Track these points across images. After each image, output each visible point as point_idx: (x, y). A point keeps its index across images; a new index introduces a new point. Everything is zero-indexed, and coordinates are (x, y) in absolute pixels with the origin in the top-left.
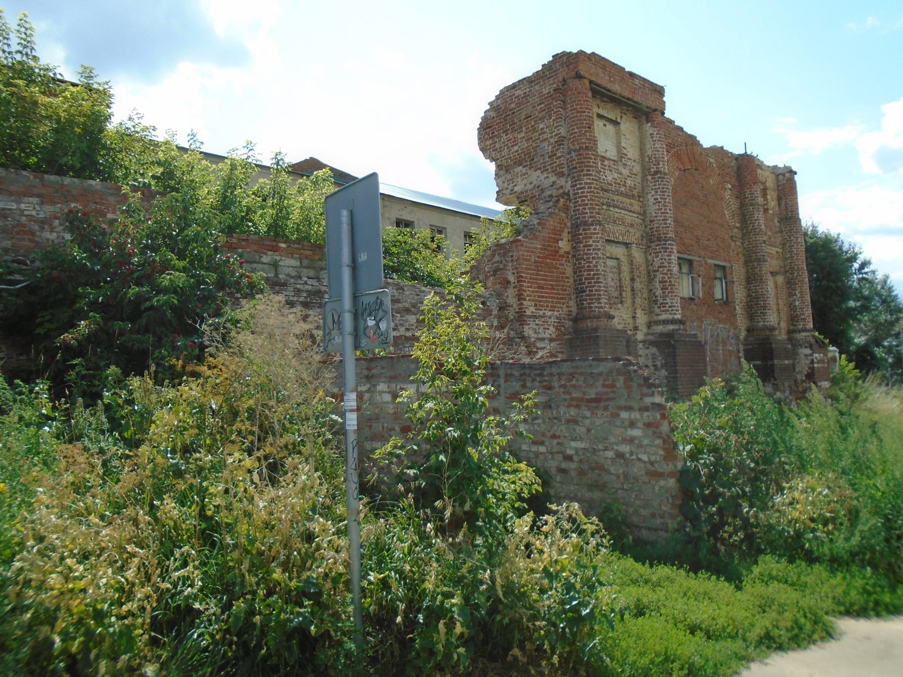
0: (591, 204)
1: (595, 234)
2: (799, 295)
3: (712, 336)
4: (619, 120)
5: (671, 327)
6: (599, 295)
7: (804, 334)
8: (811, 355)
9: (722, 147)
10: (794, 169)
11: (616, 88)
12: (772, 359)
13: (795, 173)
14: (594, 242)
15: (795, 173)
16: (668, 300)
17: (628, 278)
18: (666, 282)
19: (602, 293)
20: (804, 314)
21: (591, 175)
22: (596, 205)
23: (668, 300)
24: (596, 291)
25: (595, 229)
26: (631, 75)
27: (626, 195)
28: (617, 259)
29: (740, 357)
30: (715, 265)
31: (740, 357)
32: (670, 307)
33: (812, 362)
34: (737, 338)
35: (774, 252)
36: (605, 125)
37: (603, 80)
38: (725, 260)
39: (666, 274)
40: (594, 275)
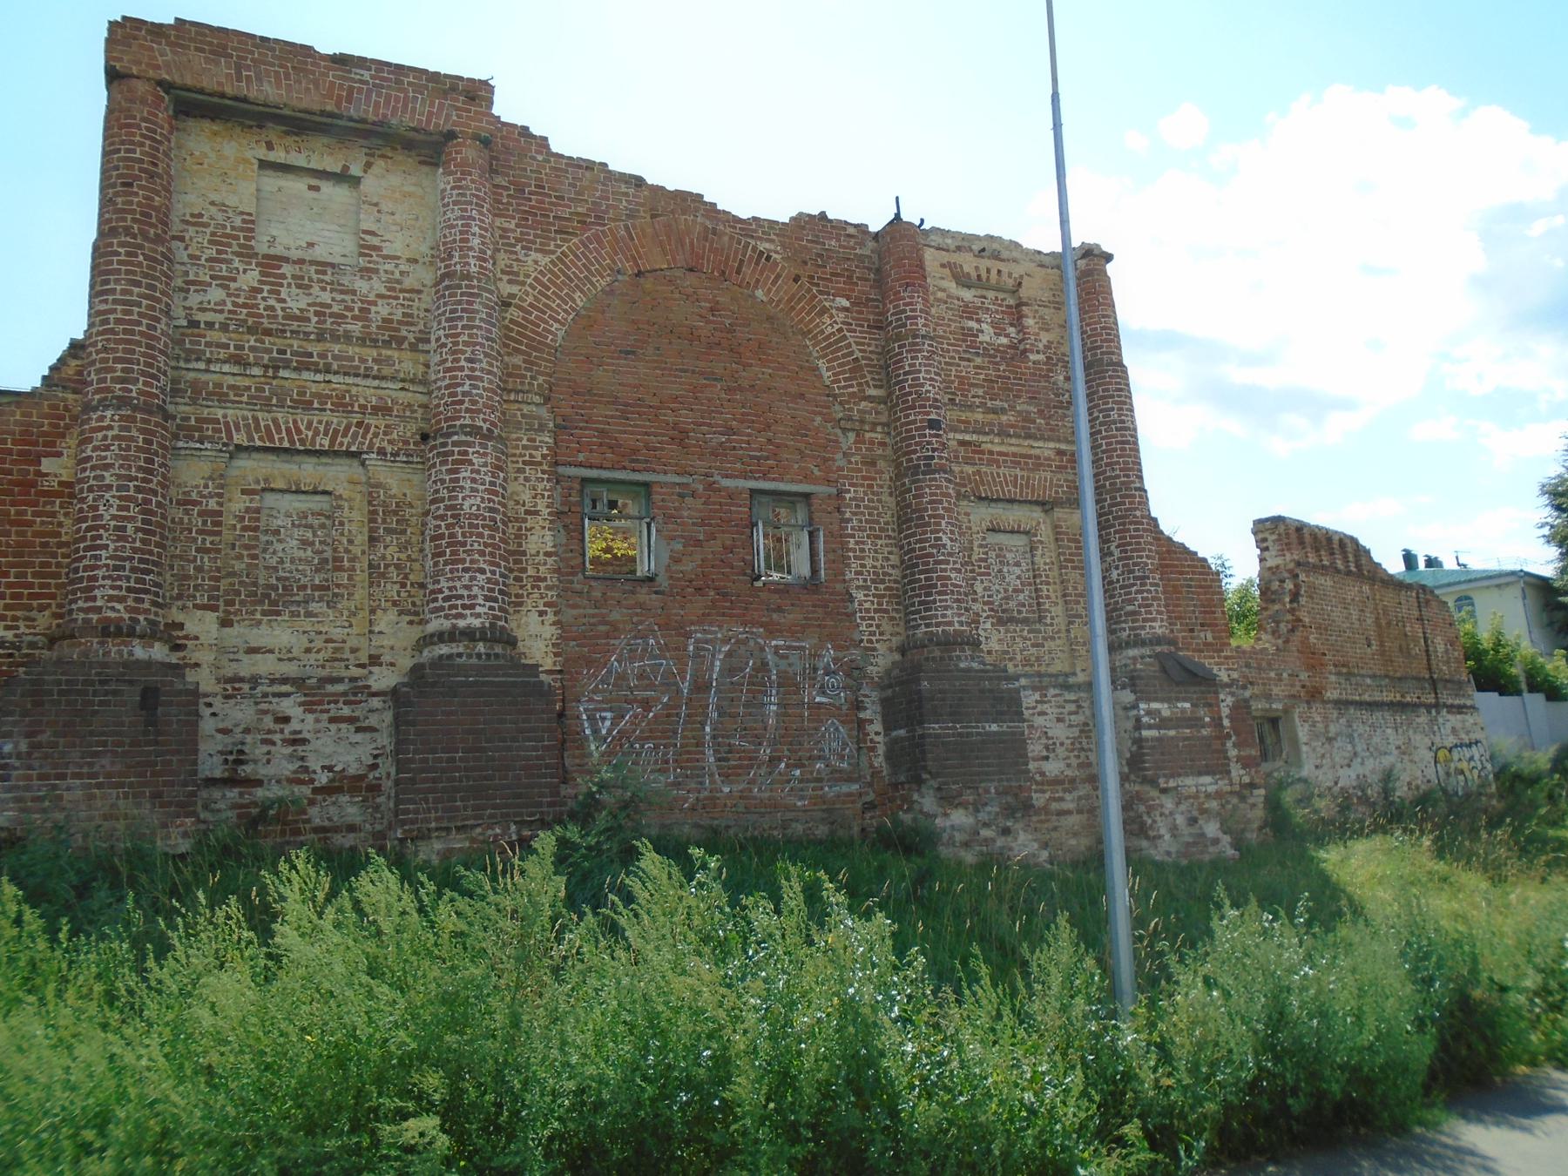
0: (106, 360)
1: (101, 429)
2: (1117, 553)
3: (730, 671)
4: (355, 170)
5: (444, 650)
6: (94, 578)
7: (1132, 652)
8: (1135, 707)
9: (823, 215)
10: (1106, 248)
11: (268, 91)
12: (921, 723)
13: (1108, 258)
14: (95, 449)
15: (1108, 258)
16: (444, 584)
17: (361, 538)
18: (442, 537)
19: (100, 573)
20: (1131, 602)
21: (113, 291)
22: (116, 360)
23: (444, 584)
24: (86, 569)
25: (102, 418)
26: (342, 60)
27: (365, 340)
28: (325, 493)
29: (861, 724)
30: (753, 492)
31: (861, 724)
32: (445, 599)
33: (1138, 725)
34: (854, 672)
35: (1051, 454)
36: (316, 189)
37: (216, 77)
38: (807, 478)
39: (442, 517)
40: (88, 529)
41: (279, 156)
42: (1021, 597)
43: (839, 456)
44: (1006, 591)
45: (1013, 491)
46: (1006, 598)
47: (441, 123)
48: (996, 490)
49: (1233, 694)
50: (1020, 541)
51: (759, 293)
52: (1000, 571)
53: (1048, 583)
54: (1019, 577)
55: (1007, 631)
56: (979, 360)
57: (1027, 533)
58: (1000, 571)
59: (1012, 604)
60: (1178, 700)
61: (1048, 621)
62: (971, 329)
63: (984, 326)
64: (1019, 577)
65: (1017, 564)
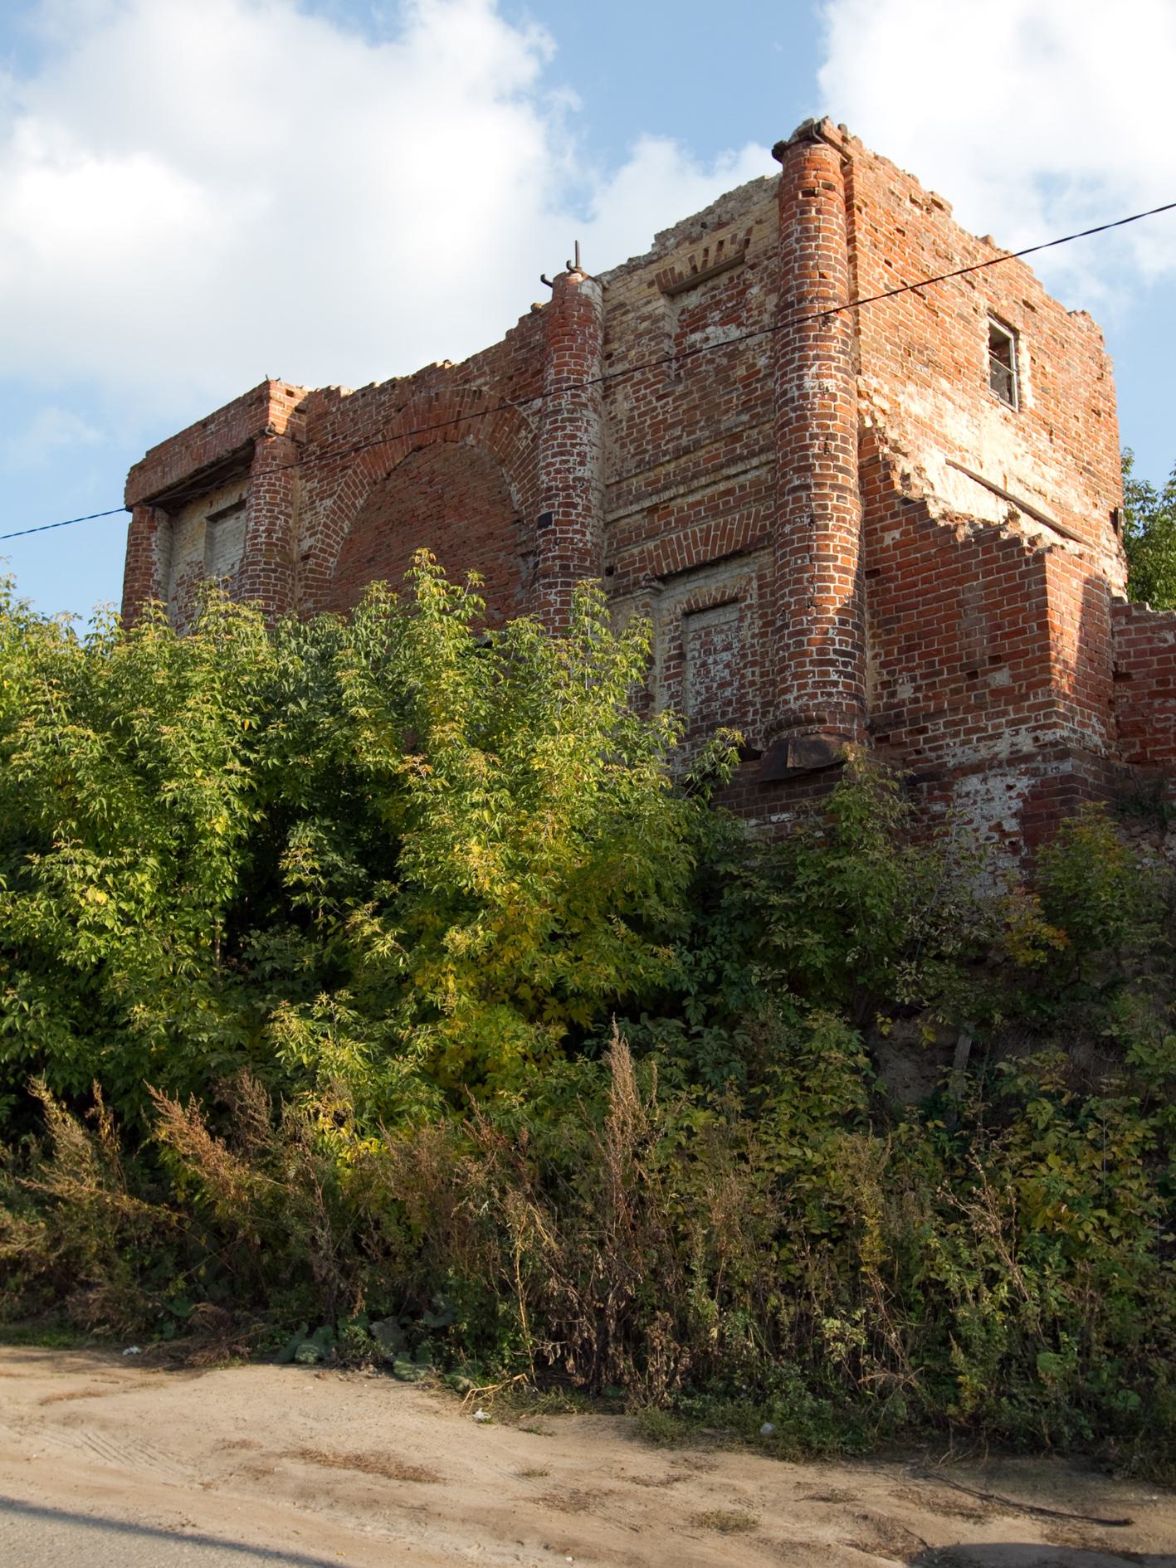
41: (216, 509)
42: (728, 692)
43: (519, 588)
44: (708, 689)
45: (704, 552)
46: (708, 700)
47: (244, 437)
48: (684, 560)
49: (1033, 773)
50: (731, 614)
51: (471, 439)
52: (704, 664)
53: (754, 664)
54: (727, 666)
55: (694, 746)
56: (680, 388)
57: (734, 600)
58: (704, 664)
59: (715, 705)
60: (773, 811)
61: (750, 718)
62: (692, 346)
63: (710, 330)
64: (727, 666)
65: (728, 648)
